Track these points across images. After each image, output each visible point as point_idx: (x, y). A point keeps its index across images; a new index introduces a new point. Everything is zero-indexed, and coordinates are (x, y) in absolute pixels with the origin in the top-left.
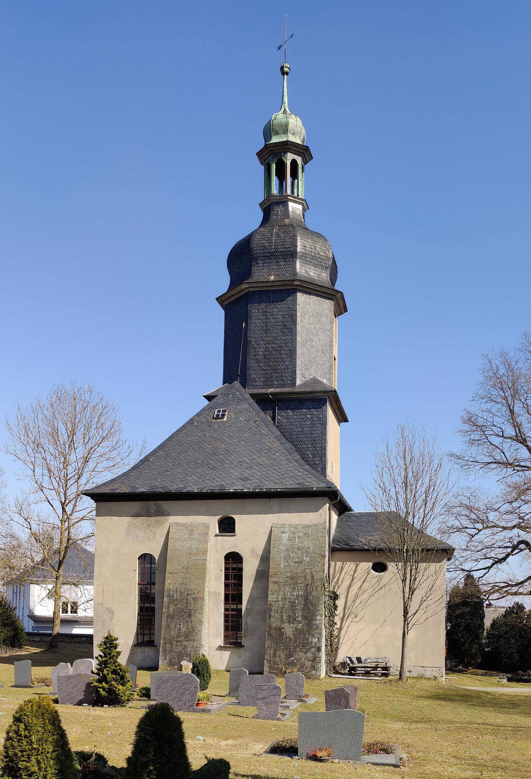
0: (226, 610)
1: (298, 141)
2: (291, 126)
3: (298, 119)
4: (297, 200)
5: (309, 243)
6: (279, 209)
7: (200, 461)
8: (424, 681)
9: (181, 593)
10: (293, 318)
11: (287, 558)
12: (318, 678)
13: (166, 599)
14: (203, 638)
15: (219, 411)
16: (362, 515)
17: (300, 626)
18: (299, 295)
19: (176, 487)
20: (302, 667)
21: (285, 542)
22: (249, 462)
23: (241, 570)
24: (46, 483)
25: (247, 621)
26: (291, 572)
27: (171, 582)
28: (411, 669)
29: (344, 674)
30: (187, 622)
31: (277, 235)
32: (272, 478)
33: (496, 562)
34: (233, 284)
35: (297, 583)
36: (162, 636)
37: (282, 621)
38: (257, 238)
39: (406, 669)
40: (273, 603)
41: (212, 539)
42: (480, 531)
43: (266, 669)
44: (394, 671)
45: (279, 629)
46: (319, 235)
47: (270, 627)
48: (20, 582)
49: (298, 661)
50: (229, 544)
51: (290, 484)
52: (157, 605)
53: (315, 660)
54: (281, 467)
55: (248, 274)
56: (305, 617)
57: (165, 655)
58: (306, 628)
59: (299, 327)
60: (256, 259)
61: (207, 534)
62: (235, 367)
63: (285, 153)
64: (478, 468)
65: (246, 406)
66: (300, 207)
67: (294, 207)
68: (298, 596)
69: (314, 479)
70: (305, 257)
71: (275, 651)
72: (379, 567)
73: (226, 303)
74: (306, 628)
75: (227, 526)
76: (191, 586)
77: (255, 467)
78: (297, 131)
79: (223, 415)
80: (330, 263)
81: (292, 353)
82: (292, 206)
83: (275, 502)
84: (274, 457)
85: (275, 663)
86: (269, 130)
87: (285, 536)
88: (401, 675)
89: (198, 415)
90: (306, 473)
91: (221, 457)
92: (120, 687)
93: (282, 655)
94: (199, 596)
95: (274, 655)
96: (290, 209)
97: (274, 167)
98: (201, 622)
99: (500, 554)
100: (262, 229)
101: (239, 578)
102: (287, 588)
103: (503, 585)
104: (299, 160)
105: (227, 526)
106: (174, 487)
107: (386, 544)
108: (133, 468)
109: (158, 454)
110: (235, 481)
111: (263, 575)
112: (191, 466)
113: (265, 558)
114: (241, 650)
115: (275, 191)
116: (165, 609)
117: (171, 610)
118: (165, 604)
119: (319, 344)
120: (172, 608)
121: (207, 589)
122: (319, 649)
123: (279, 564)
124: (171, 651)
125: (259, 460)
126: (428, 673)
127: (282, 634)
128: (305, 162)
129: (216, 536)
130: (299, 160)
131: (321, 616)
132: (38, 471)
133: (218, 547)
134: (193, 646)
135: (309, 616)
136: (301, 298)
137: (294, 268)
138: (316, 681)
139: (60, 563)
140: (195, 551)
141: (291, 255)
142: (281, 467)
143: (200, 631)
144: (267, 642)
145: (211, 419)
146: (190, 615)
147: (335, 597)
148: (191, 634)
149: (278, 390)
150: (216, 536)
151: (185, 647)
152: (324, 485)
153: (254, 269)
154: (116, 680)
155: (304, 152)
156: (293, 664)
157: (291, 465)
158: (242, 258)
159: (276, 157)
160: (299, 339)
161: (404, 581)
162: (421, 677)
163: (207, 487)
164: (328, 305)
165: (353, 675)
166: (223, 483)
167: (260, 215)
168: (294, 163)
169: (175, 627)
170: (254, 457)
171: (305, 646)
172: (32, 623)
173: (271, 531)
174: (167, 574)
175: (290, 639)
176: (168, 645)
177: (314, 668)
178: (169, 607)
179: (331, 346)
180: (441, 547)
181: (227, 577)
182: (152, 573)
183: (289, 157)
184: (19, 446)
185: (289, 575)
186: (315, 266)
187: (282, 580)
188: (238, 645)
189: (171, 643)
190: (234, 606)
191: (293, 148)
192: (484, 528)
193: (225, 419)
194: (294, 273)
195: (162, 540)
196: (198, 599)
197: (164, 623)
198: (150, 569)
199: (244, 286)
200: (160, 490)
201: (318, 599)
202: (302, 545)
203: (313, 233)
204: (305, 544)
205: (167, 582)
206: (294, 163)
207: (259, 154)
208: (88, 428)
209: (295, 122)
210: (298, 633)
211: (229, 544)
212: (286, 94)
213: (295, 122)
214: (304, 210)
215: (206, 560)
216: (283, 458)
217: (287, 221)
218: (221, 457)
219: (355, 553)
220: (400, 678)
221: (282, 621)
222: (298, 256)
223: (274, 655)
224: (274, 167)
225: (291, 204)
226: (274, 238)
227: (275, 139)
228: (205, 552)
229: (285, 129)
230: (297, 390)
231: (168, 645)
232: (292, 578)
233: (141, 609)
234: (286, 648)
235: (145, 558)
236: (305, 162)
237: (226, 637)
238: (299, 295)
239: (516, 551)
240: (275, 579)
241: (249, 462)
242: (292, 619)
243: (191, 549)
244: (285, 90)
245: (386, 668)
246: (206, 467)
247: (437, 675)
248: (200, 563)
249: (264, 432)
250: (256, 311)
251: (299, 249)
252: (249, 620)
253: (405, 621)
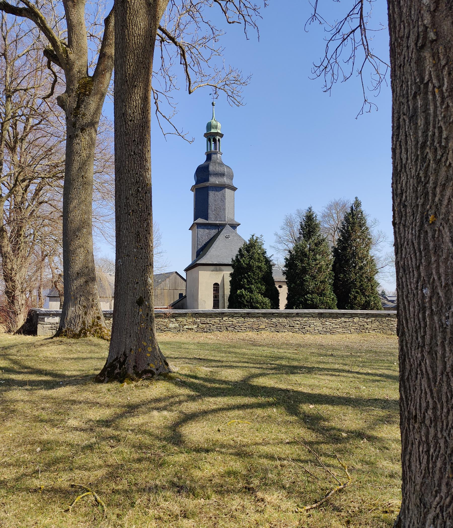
1: (219, 131)
46: (230, 168)
60: (211, 174)
86: (209, 126)
130: (220, 138)
153: (210, 178)
155: (221, 135)
158: (202, 173)
168: (219, 139)
183: (217, 138)
206: (219, 139)
209: (219, 125)
227: (213, 131)
229: (216, 127)
233: (214, 300)
235: (216, 285)
250: (212, 194)
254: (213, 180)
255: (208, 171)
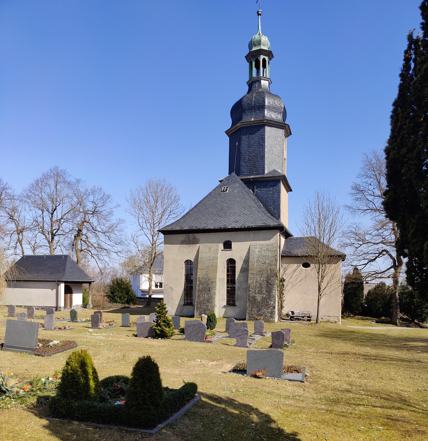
0: (228, 287)
1: (266, 48)
2: (262, 41)
3: (266, 37)
4: (266, 79)
5: (271, 101)
6: (257, 84)
7: (214, 213)
8: (329, 324)
9: (205, 279)
10: (263, 139)
11: (258, 261)
12: (273, 322)
13: (198, 282)
14: (216, 301)
15: (224, 188)
16: (297, 238)
17: (264, 296)
18: (266, 128)
19: (202, 226)
20: (265, 316)
21: (257, 253)
22: (239, 213)
23: (235, 267)
24: (144, 226)
25: (238, 293)
26: (260, 268)
27: (200, 274)
28: (322, 317)
29: (288, 320)
30: (208, 293)
31: (255, 98)
32: (250, 221)
33: (370, 261)
34: (233, 124)
35: (263, 274)
36: (196, 300)
37: (255, 293)
38: (245, 99)
39: (319, 317)
40: (251, 284)
41: (220, 252)
42: (361, 245)
43: (247, 317)
44: (314, 318)
45: (254, 297)
46: (277, 96)
47: (249, 296)
48: (137, 272)
49: (263, 313)
50: (229, 254)
51: (259, 223)
52: (194, 286)
53: (272, 313)
54: (255, 215)
55: (240, 119)
56: (267, 291)
57: (197, 310)
58: (267, 297)
59: (266, 144)
61: (218, 249)
62: (235, 166)
63: (260, 55)
64: (360, 212)
65: (238, 185)
66: (267, 82)
67: (264, 83)
68: (263, 280)
69: (272, 221)
70: (270, 108)
71: (252, 308)
72: (306, 265)
73: (230, 133)
74: (267, 297)
75: (228, 245)
76: (210, 276)
77: (242, 216)
78: (266, 43)
79: (226, 190)
80: (283, 110)
81: (263, 157)
82: (263, 82)
83: (252, 233)
84: (252, 210)
85: (252, 314)
86: (251, 44)
87: (257, 250)
88: (317, 320)
89: (214, 190)
90: (268, 218)
91: (225, 211)
92: (167, 329)
93: (255, 310)
94: (214, 280)
95: (251, 311)
96: (262, 83)
97: (254, 63)
98: (215, 293)
99: (372, 257)
100: (247, 95)
101: (234, 271)
102: (258, 277)
103: (374, 273)
104: (267, 58)
105: (228, 245)
106: (201, 227)
107: (311, 255)
108: (183, 217)
109: (194, 210)
110: (231, 223)
111: (245, 270)
112: (210, 215)
113: (247, 261)
114: (235, 307)
115: (254, 74)
116: (197, 286)
117: (200, 287)
118: (197, 285)
119: (277, 152)
120: (201, 286)
121: (218, 277)
122: (274, 308)
123: (254, 264)
124: (200, 308)
125: (244, 212)
126: (332, 319)
127: (255, 300)
128: (270, 59)
129: (222, 250)
130: (267, 58)
131: (275, 290)
132: (141, 220)
133: (223, 256)
134: (211, 306)
135: (269, 291)
136: (267, 129)
137: (264, 114)
138: (273, 324)
139: (152, 265)
140: (212, 258)
141: (262, 107)
142: (255, 215)
143: (214, 298)
144: (248, 304)
145: (220, 192)
146: (209, 291)
147: (282, 280)
148: (210, 300)
149: (256, 176)
150: (222, 250)
151: (207, 306)
152: (277, 224)
154: (165, 326)
155: (269, 54)
156: (261, 315)
157: (260, 214)
158: (238, 110)
159: (255, 58)
160: (266, 150)
161: (318, 272)
162: (328, 321)
163: (217, 226)
164: (281, 132)
165: (292, 320)
166: (226, 224)
167: (247, 88)
168: (264, 60)
169: (202, 296)
170: (242, 210)
171: (267, 306)
172: (141, 293)
173: (250, 248)
174: (198, 270)
175: (260, 302)
176: (199, 305)
177: (271, 317)
178: (199, 286)
179: (283, 153)
180: (339, 254)
181: (228, 271)
182: (191, 269)
184: (132, 208)
185: (259, 270)
186: (275, 112)
187: (255, 272)
188: (234, 305)
189: (200, 304)
190: (232, 286)
191: (263, 52)
192: (363, 244)
193: (227, 192)
194: (264, 116)
195: (196, 253)
196: (214, 282)
197: (197, 294)
198: (190, 267)
199: (238, 125)
200: (195, 228)
201: (274, 282)
202: (266, 254)
203: (273, 95)
204: (267, 254)
205: (199, 274)
206: (264, 60)
207: (246, 57)
208: (163, 198)
209: (264, 39)
210: (264, 299)
211: (229, 254)
212: (260, 25)
213: (264, 39)
214: (269, 84)
215: (217, 262)
216: (256, 211)
217: (260, 90)
218: (225, 211)
219: (293, 258)
220: (317, 322)
221: (255, 293)
222: (266, 107)
223: (251, 311)
224: (254, 63)
225: (262, 81)
226: (254, 99)
227: (254, 49)
228: (217, 259)
229: (259, 43)
230: (265, 176)
231: (199, 305)
232: (260, 271)
234: (258, 307)
235: (188, 262)
236: (270, 59)
237: (227, 301)
238: (266, 128)
239: (381, 255)
240: (252, 272)
241: (239, 213)
242: (260, 292)
243: (210, 257)
244: (260, 23)
245: (309, 317)
246: (217, 216)
247: (336, 320)
248: (215, 264)
249: (246, 197)
251: (266, 104)
252: (239, 293)
253: (319, 293)
254: (251, 118)
255: (242, 106)
